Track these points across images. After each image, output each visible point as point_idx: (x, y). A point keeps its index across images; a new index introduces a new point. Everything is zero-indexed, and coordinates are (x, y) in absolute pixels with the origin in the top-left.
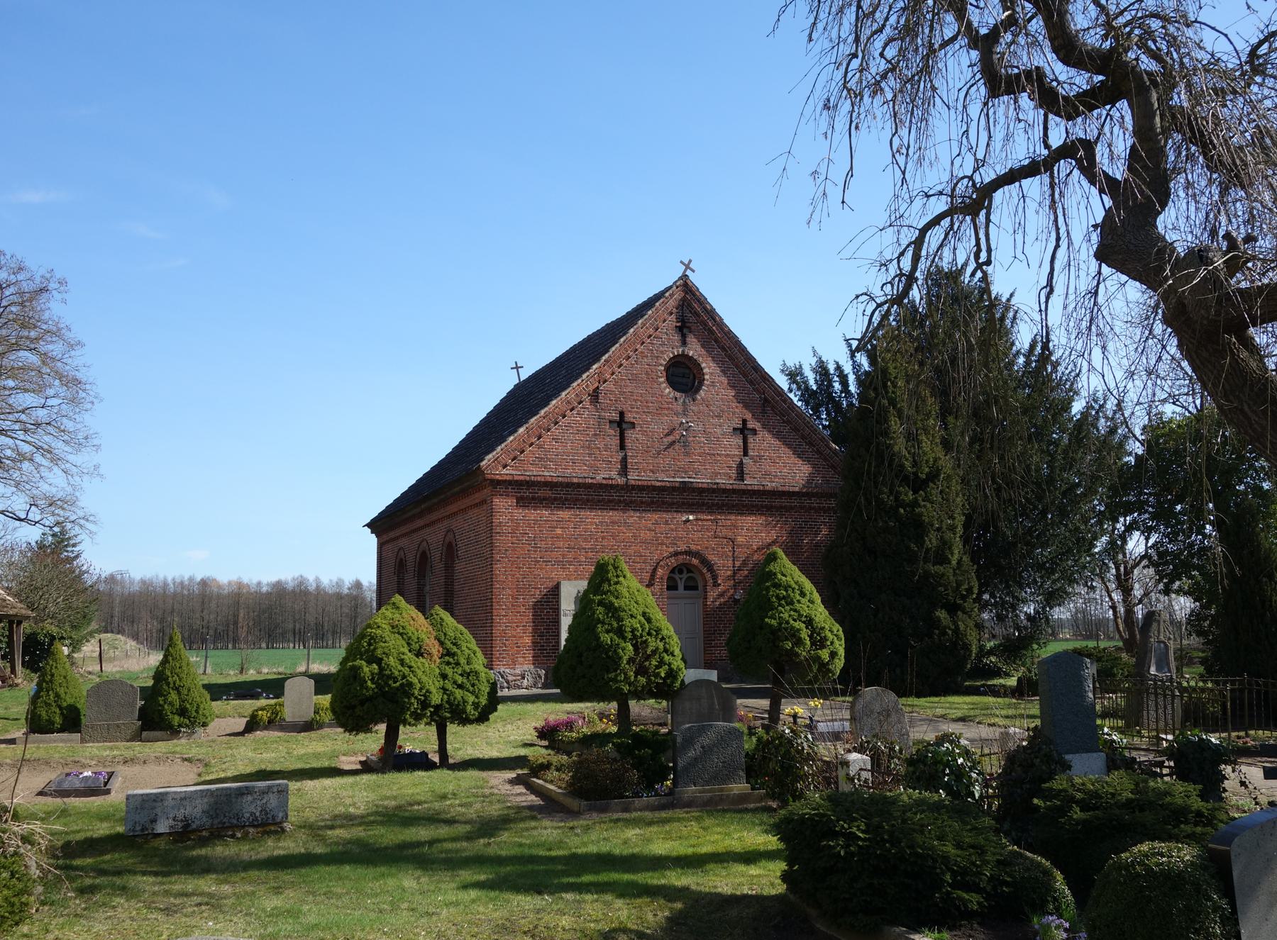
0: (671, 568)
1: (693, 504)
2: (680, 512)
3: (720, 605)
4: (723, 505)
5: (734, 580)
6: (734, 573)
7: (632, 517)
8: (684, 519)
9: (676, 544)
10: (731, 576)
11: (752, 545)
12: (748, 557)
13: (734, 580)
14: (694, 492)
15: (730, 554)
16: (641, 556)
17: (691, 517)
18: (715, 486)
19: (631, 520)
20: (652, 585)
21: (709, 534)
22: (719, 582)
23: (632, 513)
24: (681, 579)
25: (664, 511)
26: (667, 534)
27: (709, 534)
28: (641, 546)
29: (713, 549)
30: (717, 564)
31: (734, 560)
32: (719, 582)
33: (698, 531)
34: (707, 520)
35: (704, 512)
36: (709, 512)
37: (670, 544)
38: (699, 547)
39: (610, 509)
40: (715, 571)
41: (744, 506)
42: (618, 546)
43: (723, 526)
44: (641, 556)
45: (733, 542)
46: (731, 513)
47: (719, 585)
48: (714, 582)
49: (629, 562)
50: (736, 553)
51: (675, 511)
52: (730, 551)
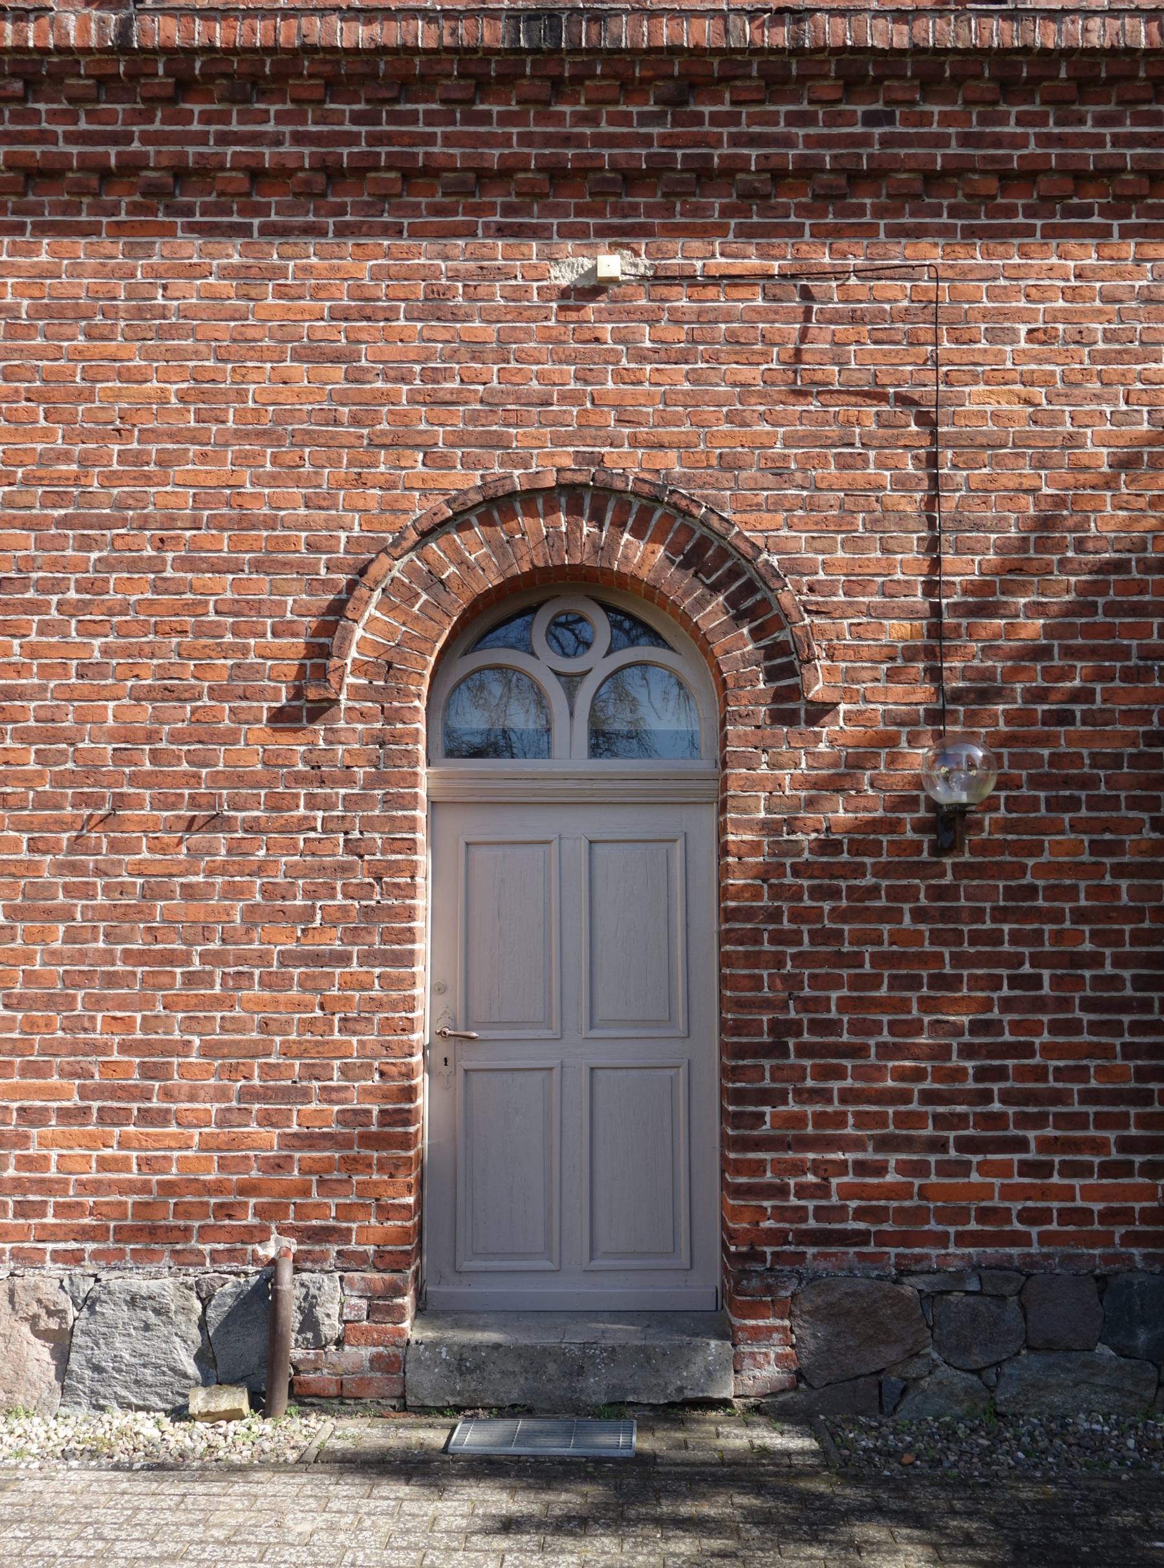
0: (458, 605)
1: (631, 179)
2: (536, 232)
3: (828, 846)
4: (856, 178)
5: (935, 674)
6: (936, 631)
7: (192, 272)
8: (563, 276)
9: (499, 442)
10: (910, 654)
11: (1072, 441)
12: (1045, 523)
13: (935, 674)
14: (629, 88)
15: (911, 504)
16: (245, 523)
17: (611, 264)
18: (781, 37)
19: (189, 294)
20: (321, 709)
21: (747, 373)
22: (817, 690)
23: (191, 248)
24: (571, 682)
25: (417, 232)
26: (431, 376)
27: (747, 373)
28: (242, 459)
29: (779, 471)
30: (795, 568)
31: (933, 546)
32: (817, 690)
33: (664, 354)
34: (735, 280)
35: (720, 230)
36: (746, 232)
37: (458, 440)
38: (671, 462)
39: (42, 229)
40: (782, 620)
41: (1007, 178)
42: (85, 461)
43: (855, 319)
44: (245, 523)
45: (924, 419)
46: (917, 233)
47: (820, 712)
48: (779, 696)
49: (155, 565)
50: (950, 502)
51: (502, 231)
52: (901, 484)
